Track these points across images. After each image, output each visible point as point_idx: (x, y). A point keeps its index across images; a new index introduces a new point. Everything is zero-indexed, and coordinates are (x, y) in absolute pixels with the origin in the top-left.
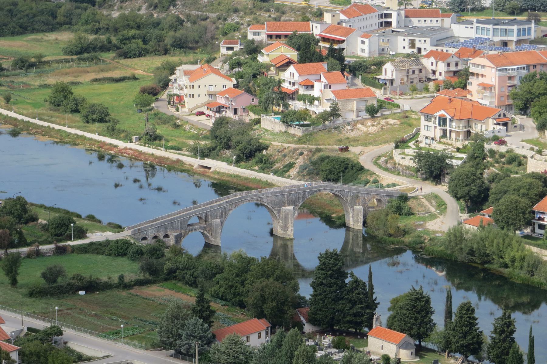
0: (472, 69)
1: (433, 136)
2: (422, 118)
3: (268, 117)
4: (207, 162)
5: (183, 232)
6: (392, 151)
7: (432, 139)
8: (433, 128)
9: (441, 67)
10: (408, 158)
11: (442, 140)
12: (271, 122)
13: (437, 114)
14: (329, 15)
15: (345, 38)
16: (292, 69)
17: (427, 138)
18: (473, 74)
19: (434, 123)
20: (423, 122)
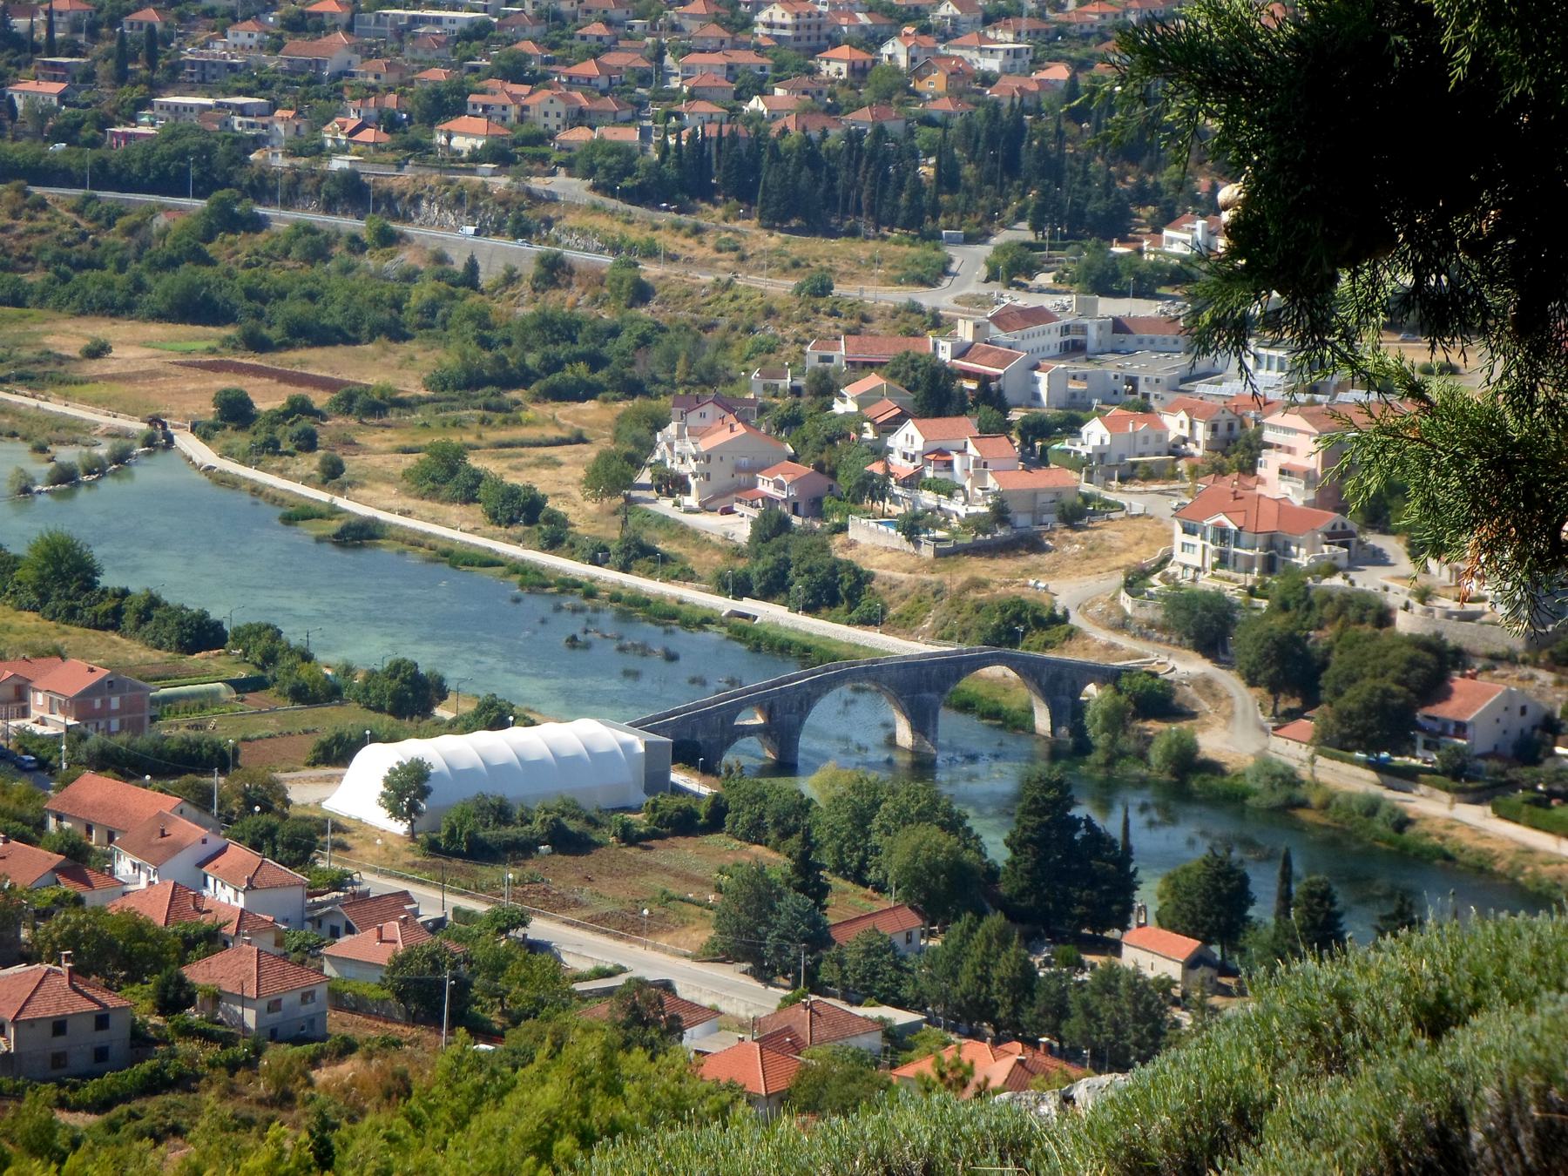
0: (1269, 436)
2: (1178, 529)
3: (864, 521)
4: (747, 605)
5: (726, 737)
6: (1118, 593)
7: (1197, 570)
8: (1199, 550)
9: (1202, 432)
10: (1150, 604)
11: (1219, 572)
12: (871, 530)
13: (1209, 522)
14: (970, 325)
15: (1001, 371)
16: (910, 427)
17: (1185, 567)
18: (1269, 446)
19: (1203, 538)
20: (1180, 537)
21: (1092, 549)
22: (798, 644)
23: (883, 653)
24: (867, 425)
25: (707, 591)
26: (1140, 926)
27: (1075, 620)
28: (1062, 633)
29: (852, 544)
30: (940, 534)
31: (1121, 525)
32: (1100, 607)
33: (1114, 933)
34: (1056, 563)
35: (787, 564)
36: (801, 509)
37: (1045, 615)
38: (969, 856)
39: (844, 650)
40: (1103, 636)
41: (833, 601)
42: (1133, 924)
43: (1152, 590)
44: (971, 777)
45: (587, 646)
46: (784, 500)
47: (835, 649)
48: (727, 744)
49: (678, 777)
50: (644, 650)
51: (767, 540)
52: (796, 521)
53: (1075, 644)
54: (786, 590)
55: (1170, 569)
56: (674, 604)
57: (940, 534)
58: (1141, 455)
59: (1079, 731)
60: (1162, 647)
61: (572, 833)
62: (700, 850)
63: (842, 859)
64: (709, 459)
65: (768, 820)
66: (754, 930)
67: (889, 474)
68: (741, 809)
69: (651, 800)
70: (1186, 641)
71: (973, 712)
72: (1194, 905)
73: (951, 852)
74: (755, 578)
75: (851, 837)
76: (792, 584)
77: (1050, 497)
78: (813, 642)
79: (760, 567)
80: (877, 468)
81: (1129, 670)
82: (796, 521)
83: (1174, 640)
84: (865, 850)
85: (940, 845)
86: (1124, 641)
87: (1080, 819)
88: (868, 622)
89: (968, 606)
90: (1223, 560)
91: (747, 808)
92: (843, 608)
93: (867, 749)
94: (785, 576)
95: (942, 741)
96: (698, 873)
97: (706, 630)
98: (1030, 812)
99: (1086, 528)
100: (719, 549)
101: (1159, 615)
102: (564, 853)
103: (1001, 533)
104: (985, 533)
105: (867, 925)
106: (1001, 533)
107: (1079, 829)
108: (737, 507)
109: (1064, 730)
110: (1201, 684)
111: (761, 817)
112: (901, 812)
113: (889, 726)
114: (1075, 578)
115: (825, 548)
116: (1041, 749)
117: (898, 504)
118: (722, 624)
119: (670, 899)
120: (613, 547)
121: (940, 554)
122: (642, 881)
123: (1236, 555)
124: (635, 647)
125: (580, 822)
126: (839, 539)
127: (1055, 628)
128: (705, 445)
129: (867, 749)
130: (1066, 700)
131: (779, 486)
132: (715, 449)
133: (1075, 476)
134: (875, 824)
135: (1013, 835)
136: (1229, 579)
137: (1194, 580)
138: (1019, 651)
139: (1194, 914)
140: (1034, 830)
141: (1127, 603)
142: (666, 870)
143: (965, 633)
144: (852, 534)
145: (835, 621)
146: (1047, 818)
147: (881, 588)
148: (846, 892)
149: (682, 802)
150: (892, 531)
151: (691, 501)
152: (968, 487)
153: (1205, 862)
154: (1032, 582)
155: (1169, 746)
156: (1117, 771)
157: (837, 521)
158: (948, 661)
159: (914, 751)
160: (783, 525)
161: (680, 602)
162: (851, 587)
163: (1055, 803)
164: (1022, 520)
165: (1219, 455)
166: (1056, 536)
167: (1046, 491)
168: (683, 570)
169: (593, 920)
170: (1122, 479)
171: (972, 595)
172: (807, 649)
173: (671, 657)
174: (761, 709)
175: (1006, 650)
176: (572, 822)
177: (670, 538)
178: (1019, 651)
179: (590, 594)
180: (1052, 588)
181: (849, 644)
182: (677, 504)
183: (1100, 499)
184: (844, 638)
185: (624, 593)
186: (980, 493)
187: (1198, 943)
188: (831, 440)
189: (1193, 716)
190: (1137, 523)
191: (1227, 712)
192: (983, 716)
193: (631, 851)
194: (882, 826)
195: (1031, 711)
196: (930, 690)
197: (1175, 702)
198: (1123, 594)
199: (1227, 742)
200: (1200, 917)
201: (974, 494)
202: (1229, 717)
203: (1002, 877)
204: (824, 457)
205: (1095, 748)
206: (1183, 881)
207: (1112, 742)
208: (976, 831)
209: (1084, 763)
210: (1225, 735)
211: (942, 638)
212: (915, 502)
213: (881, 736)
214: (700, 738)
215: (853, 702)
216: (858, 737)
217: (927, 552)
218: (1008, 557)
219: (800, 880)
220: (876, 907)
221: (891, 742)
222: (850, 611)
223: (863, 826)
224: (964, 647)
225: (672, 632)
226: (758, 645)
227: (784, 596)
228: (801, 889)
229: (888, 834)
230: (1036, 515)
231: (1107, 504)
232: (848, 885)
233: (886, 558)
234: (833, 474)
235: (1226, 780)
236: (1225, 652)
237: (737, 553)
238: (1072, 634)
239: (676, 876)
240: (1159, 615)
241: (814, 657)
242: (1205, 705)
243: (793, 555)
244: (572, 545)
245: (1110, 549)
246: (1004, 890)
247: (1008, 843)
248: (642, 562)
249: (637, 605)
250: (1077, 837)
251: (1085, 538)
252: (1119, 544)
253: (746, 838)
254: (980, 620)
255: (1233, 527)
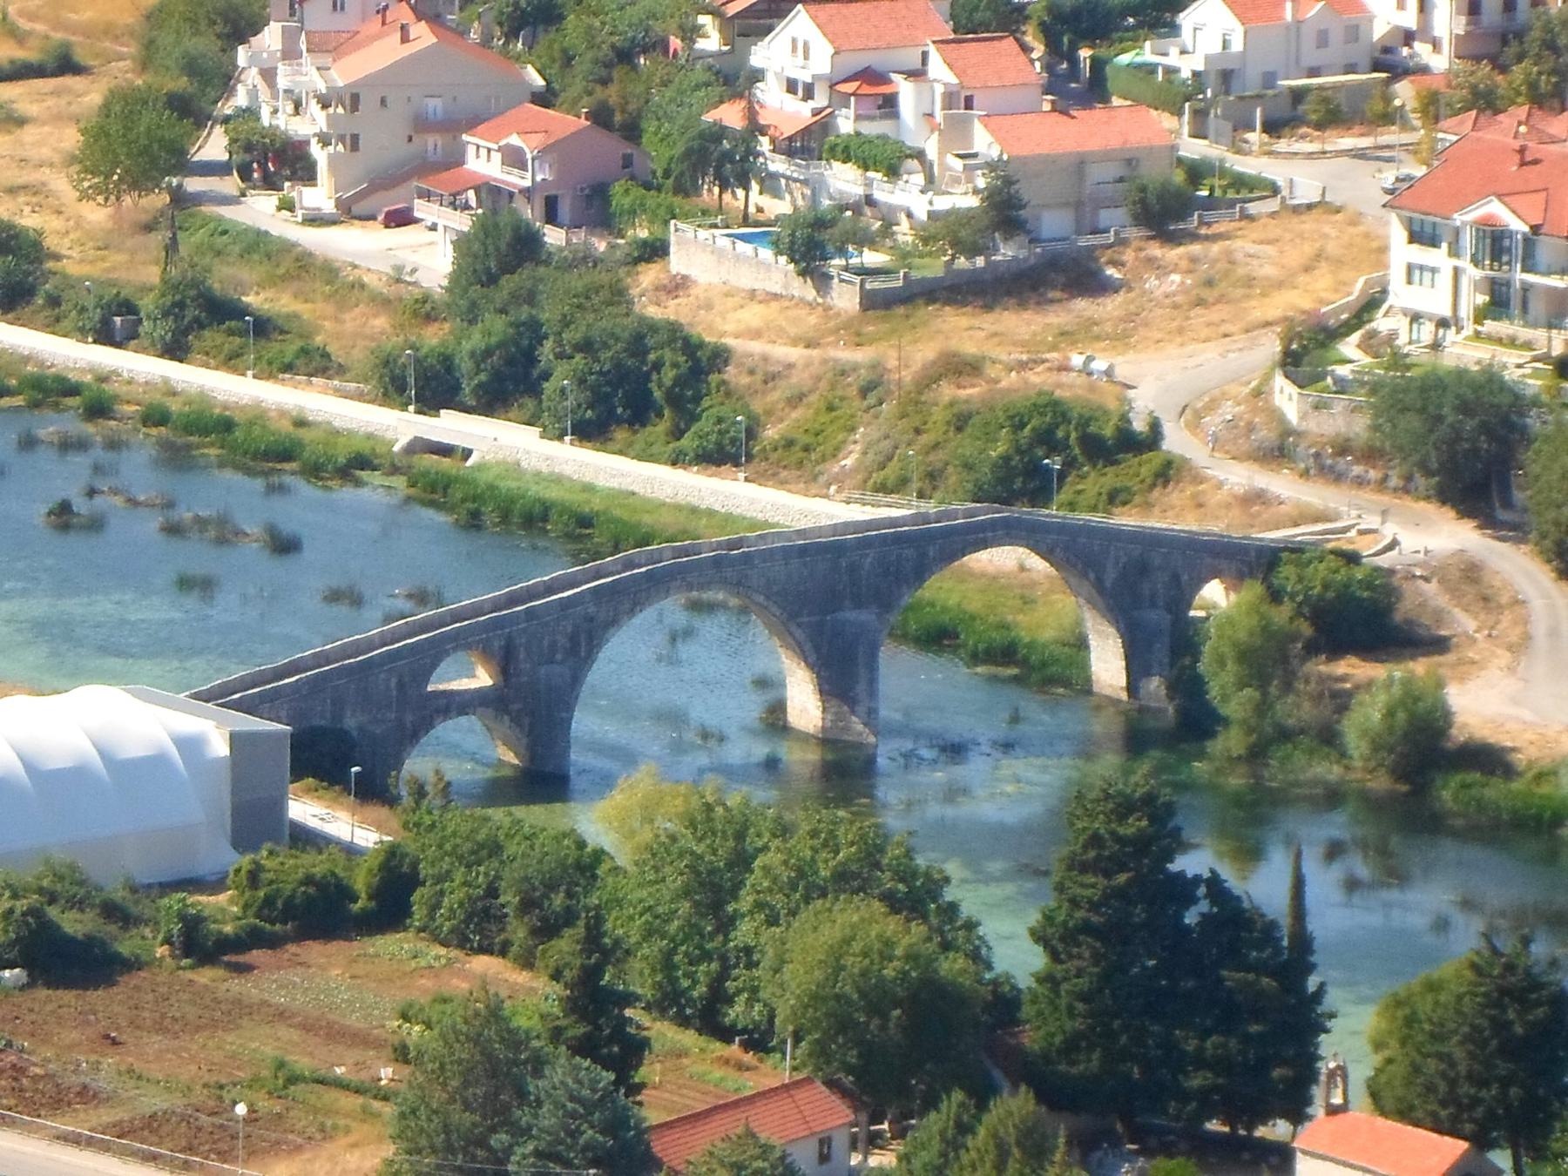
1: (1447, 312)
2: (1397, 233)
3: (703, 234)
4: (450, 426)
5: (409, 718)
6: (1267, 378)
7: (1443, 323)
8: (1445, 279)
10: (1340, 404)
11: (1490, 326)
12: (719, 254)
13: (1465, 218)
16: (800, 23)
17: (1416, 318)
19: (1454, 252)
20: (1402, 251)
21: (1209, 283)
22: (565, 509)
23: (754, 525)
24: (705, 20)
25: (360, 397)
26: (1333, 1111)
27: (1176, 441)
28: (1145, 471)
29: (679, 286)
30: (872, 258)
31: (1273, 229)
32: (1228, 410)
33: (1278, 1130)
34: (1130, 317)
35: (534, 332)
36: (565, 210)
37: (1108, 432)
38: (951, 966)
39: (666, 520)
40: (1239, 476)
41: (640, 412)
42: (1318, 1110)
43: (1343, 371)
44: (953, 793)
45: (96, 524)
46: (527, 193)
47: (647, 519)
48: (411, 735)
49: (305, 809)
50: (224, 532)
51: (491, 280)
52: (554, 237)
53: (1176, 496)
54: (534, 390)
55: (1382, 323)
56: (286, 426)
57: (872, 258)
58: (1314, 72)
59: (1188, 687)
60: (1368, 496)
61: (71, 940)
62: (360, 969)
63: (673, 981)
64: (355, 99)
65: (509, 898)
66: (482, 1142)
67: (755, 128)
68: (446, 876)
69: (246, 861)
70: (1421, 481)
71: (954, 649)
72: (1452, 1064)
73: (911, 957)
74: (465, 365)
75: (692, 930)
76: (546, 376)
77: (1112, 170)
78: (597, 504)
79: (475, 340)
80: (731, 115)
81: (1296, 549)
82: (554, 237)
83: (1394, 481)
84: (723, 959)
85: (888, 944)
86: (1283, 485)
87: (1197, 879)
88: (718, 456)
89: (939, 415)
90: (1499, 302)
91: (459, 876)
92: (661, 427)
93: (722, 739)
94: (530, 359)
95: (886, 712)
96: (354, 1021)
97: (358, 483)
98: (1084, 868)
99: (1194, 237)
100: (383, 303)
101: (1359, 427)
102: (51, 984)
103: (1007, 252)
104: (972, 252)
105: (732, 1124)
106: (1007, 252)
107: (1194, 901)
108: (421, 209)
109: (1155, 685)
110: (1455, 574)
111: (492, 892)
112: (801, 874)
113: (768, 684)
114: (1172, 349)
115: (618, 295)
116: (1106, 726)
117: (776, 194)
118: (395, 470)
119: (293, 1080)
120: (147, 304)
121: (873, 302)
122: (232, 1041)
123: (1526, 288)
124: (201, 523)
125: (90, 915)
126: (649, 275)
127: (1131, 461)
128: (346, 72)
129: (722, 739)
130: (1157, 617)
131: (514, 159)
132: (369, 81)
133: (1167, 121)
134: (746, 901)
135: (1048, 918)
136: (1512, 343)
137: (1436, 346)
138: (1052, 513)
139: (1453, 1083)
140: (1094, 906)
141: (1287, 399)
142: (282, 1015)
143: (933, 477)
144: (678, 262)
145: (640, 458)
146: (1122, 878)
147: (745, 380)
148: (681, 1053)
149: (316, 864)
150: (766, 253)
151: (319, 196)
152: (932, 153)
153: (1474, 966)
154: (1077, 360)
155: (1390, 713)
156: (1274, 774)
157: (643, 234)
158: (898, 539)
159: (826, 740)
160: (526, 246)
161: (301, 423)
162: (677, 381)
163: (1141, 845)
164: (1054, 223)
165: (1485, 68)
166: (1129, 256)
167: (1106, 156)
168: (304, 352)
169: (123, 1130)
170: (1273, 128)
171: (947, 391)
172: (585, 521)
173: (284, 545)
174: (487, 654)
175: (1022, 511)
176: (73, 915)
177: (271, 282)
178: (1052, 513)
179: (99, 409)
180: (1121, 373)
181: (678, 508)
182: (287, 205)
183: (1223, 172)
184: (664, 494)
185: (174, 406)
186: (958, 164)
187: (1463, 1145)
188: (625, 56)
189: (1439, 645)
190: (1308, 224)
191: (1514, 635)
192: (975, 658)
193: (206, 976)
194: (759, 906)
195: (1081, 644)
196: (859, 604)
197: (1398, 617)
198: (1280, 381)
199: (1515, 701)
200: (1466, 1089)
201: (945, 167)
202: (1520, 647)
203: (1027, 1011)
204: (612, 94)
205: (1225, 722)
206: (1425, 1007)
207: (1263, 708)
208: (967, 910)
209: (1201, 755)
210: (1510, 685)
211: (882, 488)
212: (815, 187)
213: (752, 708)
214: (351, 722)
215: (688, 633)
216: (702, 712)
217: (846, 298)
218: (1022, 305)
219: (581, 1030)
220: (751, 1084)
221: (775, 720)
222: (677, 433)
223: (716, 906)
224: (930, 507)
225: (281, 489)
226: (475, 515)
227: (530, 403)
228: (583, 1048)
229: (773, 921)
230: (1085, 211)
231: (1241, 182)
232: (689, 1038)
233: (753, 315)
234: (632, 132)
235: (1516, 785)
236: (1508, 504)
237: (424, 310)
238: (1168, 473)
239: (307, 1027)
240: (1359, 427)
241: (600, 538)
242: (1464, 622)
243: (548, 314)
244: (54, 301)
245: (1249, 282)
246: (1031, 1038)
247: (1038, 936)
248: (212, 337)
249: (204, 431)
250: (1191, 918)
251: (1194, 260)
252: (1269, 270)
253: (459, 939)
254: (966, 445)
255: (1518, 226)
